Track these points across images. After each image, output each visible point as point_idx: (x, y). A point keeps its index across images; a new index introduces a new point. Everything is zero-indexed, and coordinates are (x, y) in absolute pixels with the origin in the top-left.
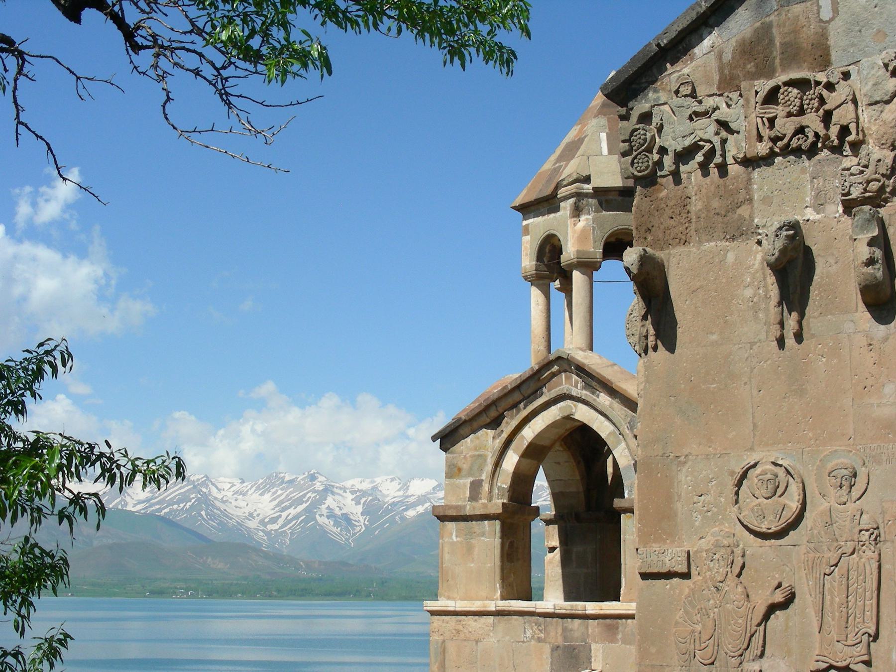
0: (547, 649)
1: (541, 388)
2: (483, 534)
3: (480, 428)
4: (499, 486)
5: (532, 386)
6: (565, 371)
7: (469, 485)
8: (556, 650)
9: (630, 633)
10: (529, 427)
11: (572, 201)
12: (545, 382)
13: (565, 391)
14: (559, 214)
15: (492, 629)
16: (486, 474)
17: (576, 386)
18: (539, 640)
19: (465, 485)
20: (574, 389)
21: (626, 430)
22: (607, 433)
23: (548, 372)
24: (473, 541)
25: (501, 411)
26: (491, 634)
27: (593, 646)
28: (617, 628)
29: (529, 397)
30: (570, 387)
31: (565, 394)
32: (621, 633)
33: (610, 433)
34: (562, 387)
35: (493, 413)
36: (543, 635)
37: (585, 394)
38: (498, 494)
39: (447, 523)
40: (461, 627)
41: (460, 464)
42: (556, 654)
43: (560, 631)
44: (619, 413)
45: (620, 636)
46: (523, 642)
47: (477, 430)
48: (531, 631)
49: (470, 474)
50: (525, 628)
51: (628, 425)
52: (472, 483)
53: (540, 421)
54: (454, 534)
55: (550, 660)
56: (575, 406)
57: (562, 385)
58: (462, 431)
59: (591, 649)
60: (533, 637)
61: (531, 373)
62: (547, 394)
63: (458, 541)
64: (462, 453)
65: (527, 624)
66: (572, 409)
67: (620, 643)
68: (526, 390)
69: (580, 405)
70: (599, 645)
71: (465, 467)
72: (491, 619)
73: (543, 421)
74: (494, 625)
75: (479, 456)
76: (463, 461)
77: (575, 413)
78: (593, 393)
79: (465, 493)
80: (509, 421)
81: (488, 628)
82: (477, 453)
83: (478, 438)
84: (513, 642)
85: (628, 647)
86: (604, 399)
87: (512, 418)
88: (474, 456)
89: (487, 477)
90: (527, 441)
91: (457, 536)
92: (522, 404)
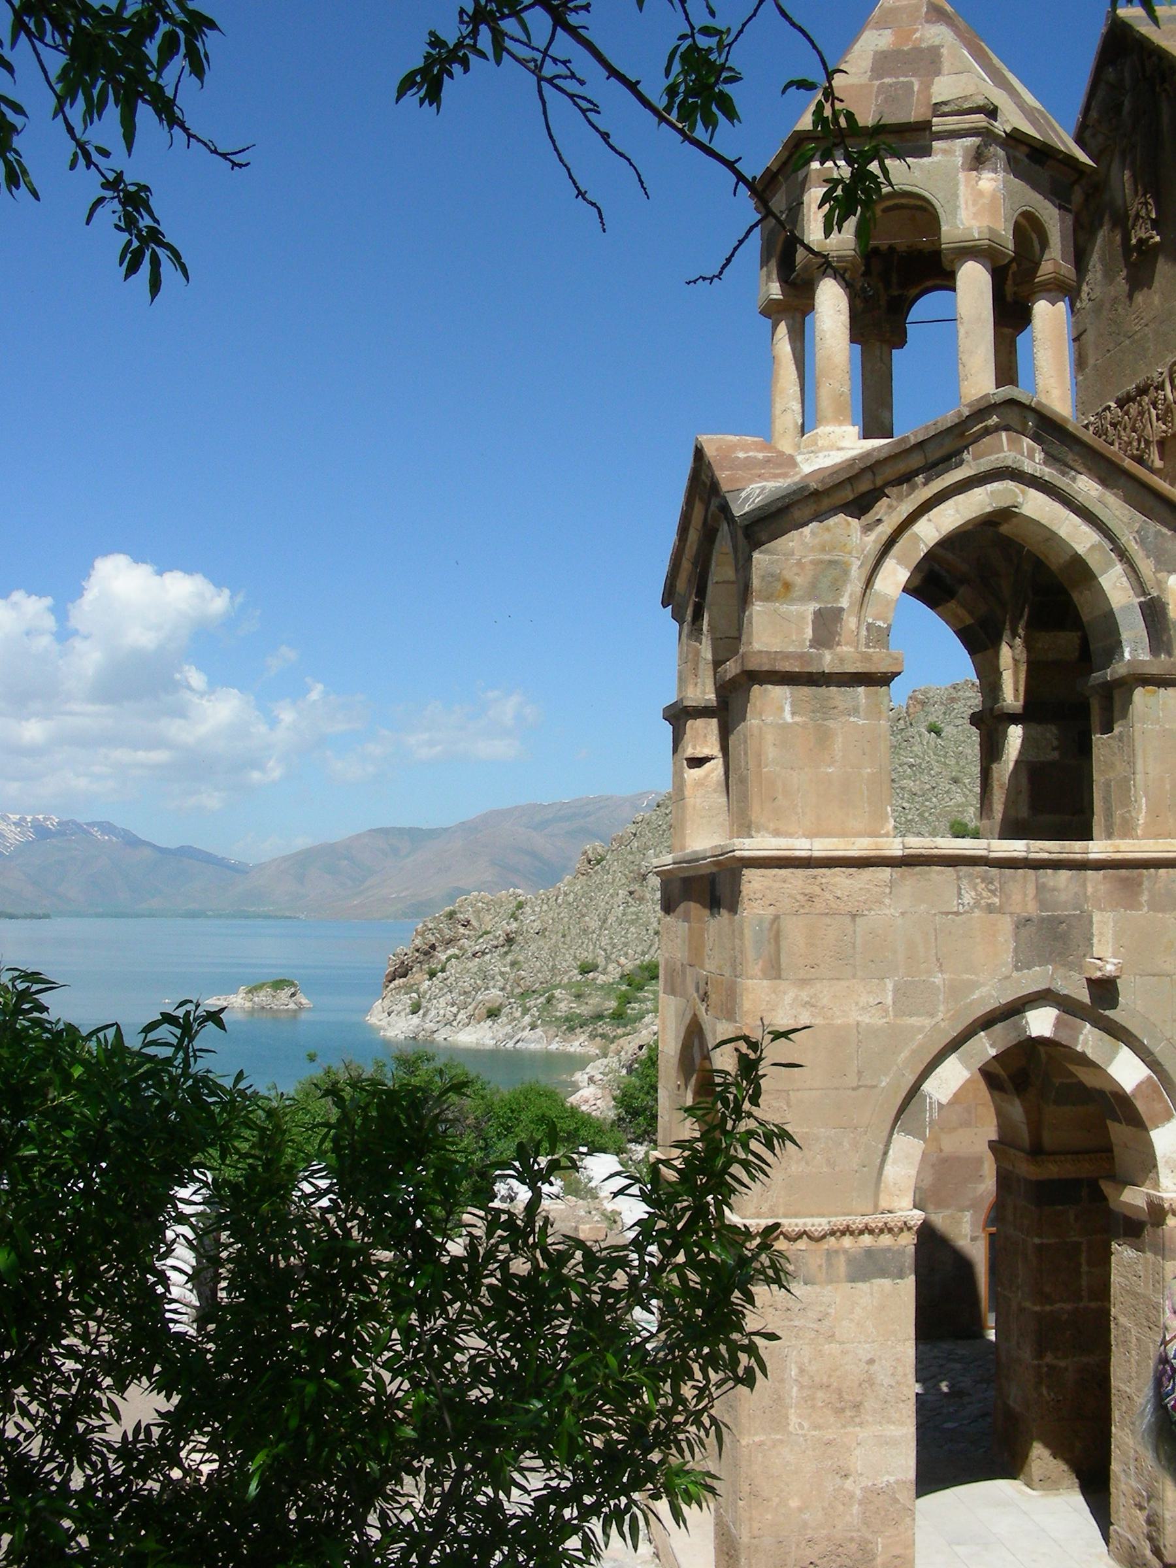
0: (1006, 924)
1: (959, 452)
2: (855, 711)
3: (834, 511)
4: (869, 624)
5: (949, 445)
6: (1007, 428)
7: (810, 617)
8: (1025, 925)
9: (1163, 891)
10: (929, 520)
11: (976, 140)
12: (971, 440)
13: (1009, 463)
14: (925, 160)
15: (887, 890)
16: (851, 597)
17: (1031, 458)
18: (990, 909)
19: (802, 618)
20: (1027, 461)
21: (1133, 543)
22: (1088, 546)
23: (981, 425)
24: (831, 724)
25: (879, 482)
26: (887, 901)
27: (1097, 917)
28: (1140, 884)
29: (935, 465)
30: (1019, 457)
31: (1007, 467)
32: (1146, 893)
33: (1093, 547)
34: (1002, 455)
35: (864, 486)
36: (997, 900)
37: (1048, 473)
38: (868, 637)
39: (769, 687)
40: (817, 890)
41: (788, 575)
42: (1024, 932)
43: (1031, 890)
44: (1117, 513)
45: (1145, 898)
46: (957, 913)
47: (825, 513)
48: (973, 893)
49: (812, 593)
50: (960, 888)
51: (1135, 535)
52: (818, 614)
53: (951, 512)
54: (788, 708)
55: (1013, 945)
56: (1023, 492)
57: (1002, 450)
58: (797, 514)
59: (1091, 922)
60: (977, 904)
61: (957, 421)
62: (972, 463)
63: (797, 724)
64: (793, 554)
65: (965, 881)
66: (1017, 496)
67: (1146, 909)
68: (935, 454)
69: (1033, 493)
70: (1109, 915)
71: (800, 581)
72: (886, 873)
73: (957, 511)
74: (892, 884)
75: (831, 562)
76: (795, 570)
77: (1022, 504)
78: (1064, 474)
79: (801, 631)
80: (895, 503)
81: (878, 889)
82: (827, 557)
83: (828, 529)
84: (935, 915)
85: (1160, 915)
86: (1086, 487)
87: (900, 499)
88: (822, 562)
89: (852, 604)
90: (926, 545)
91: (793, 714)
92: (920, 479)
